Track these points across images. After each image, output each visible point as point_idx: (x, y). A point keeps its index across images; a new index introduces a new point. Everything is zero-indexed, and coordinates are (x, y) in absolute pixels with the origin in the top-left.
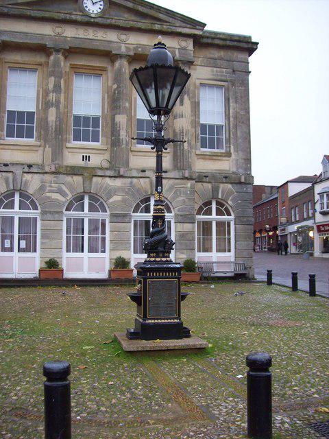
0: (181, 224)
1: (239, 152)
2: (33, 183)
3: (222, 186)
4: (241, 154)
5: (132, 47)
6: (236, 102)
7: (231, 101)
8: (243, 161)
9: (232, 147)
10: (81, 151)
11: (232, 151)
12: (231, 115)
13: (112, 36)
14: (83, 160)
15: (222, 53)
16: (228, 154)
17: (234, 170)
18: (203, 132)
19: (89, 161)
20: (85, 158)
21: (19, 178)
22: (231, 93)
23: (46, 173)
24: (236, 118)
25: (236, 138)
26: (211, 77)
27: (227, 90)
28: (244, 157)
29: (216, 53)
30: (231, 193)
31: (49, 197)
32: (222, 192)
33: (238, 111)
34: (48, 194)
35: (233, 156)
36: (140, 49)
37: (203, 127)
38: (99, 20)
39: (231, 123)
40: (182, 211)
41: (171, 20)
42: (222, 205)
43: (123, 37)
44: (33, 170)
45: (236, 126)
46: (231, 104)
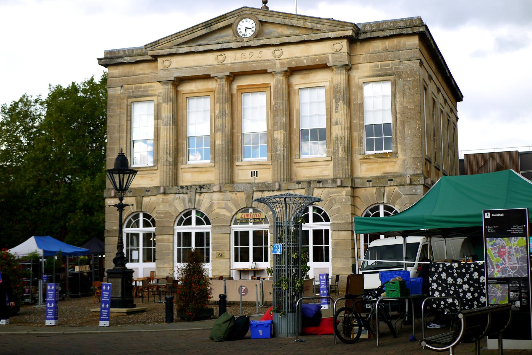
0: (337, 232)
1: (407, 151)
2: (205, 202)
3: (387, 189)
4: (409, 152)
5: (285, 61)
6: (404, 96)
7: (398, 96)
8: (412, 160)
9: (399, 146)
10: (249, 167)
11: (399, 151)
12: (397, 111)
13: (267, 54)
14: (252, 176)
15: (387, 43)
16: (394, 155)
17: (402, 171)
18: (369, 134)
19: (257, 176)
20: (254, 174)
21: (193, 198)
22: (398, 88)
23: (214, 192)
24: (403, 113)
25: (403, 138)
26: (375, 73)
27: (394, 85)
28: (413, 156)
29: (378, 45)
30: (398, 196)
31: (217, 214)
32: (388, 199)
33: (406, 105)
34: (217, 211)
35: (400, 156)
36: (293, 63)
37: (369, 127)
38: (252, 43)
39: (398, 121)
40: (337, 220)
41: (319, 26)
42: (391, 209)
43: (278, 53)
44: (203, 190)
45: (403, 123)
46: (398, 100)
